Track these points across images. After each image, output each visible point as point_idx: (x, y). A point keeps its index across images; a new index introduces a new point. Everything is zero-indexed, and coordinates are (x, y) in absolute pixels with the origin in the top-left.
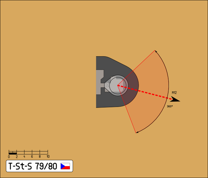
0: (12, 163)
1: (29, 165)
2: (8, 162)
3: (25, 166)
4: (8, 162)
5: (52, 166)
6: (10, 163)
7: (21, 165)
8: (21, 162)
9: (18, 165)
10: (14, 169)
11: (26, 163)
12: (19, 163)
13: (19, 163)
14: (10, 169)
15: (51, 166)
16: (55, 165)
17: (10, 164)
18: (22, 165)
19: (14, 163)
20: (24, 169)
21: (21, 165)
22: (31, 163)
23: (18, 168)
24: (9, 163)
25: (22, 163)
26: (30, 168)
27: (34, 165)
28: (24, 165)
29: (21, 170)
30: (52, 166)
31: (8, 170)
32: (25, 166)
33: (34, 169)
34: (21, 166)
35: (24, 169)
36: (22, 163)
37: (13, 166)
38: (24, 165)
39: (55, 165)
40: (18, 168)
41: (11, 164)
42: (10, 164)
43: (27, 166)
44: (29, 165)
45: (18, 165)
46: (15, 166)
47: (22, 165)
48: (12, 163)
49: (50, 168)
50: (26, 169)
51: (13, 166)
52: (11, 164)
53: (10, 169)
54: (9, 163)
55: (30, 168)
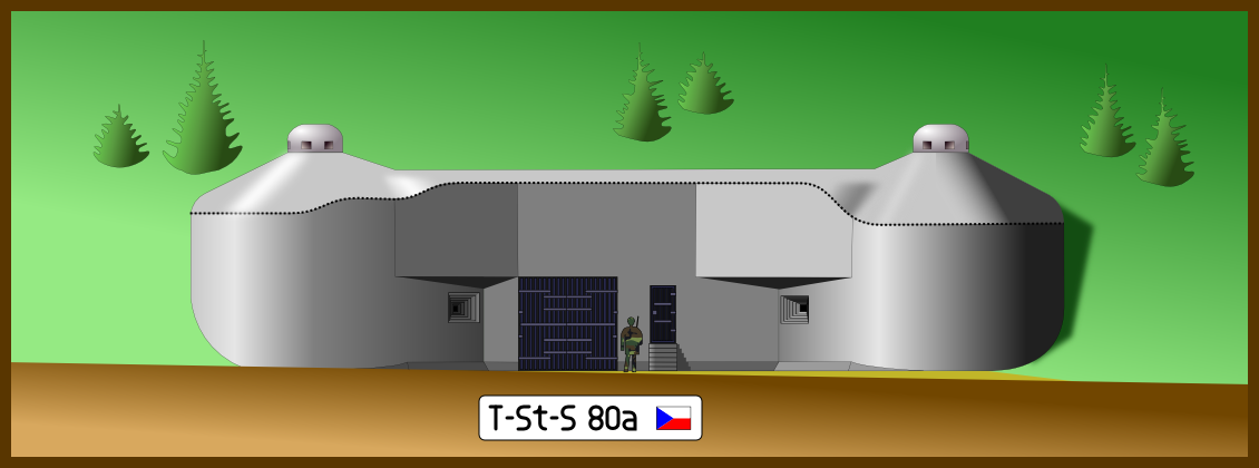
0: (501, 407)
1: (567, 412)
2: (486, 402)
3: (552, 418)
4: (486, 402)
5: (604, 418)
6: (496, 408)
7: (535, 412)
8: (535, 402)
9: (523, 412)
10: (508, 430)
11: (553, 404)
12: (529, 407)
13: (529, 407)
14: (496, 429)
15: (599, 418)
16: (613, 413)
17: (493, 410)
18: (540, 412)
19: (510, 404)
20: (545, 429)
21: (535, 412)
22: (574, 407)
23: (525, 424)
24: (490, 407)
25: (540, 407)
26: (569, 424)
27: (581, 416)
28: (546, 412)
29: (534, 433)
30: (604, 418)
31: (487, 431)
32: (552, 418)
33: (582, 431)
34: (534, 419)
35: (545, 429)
36: (540, 407)
37: (507, 418)
38: (546, 412)
39: (613, 413)
40: (525, 424)
41: (499, 410)
42: (493, 410)
43: (557, 418)
44: (567, 412)
45: (523, 412)
46: (512, 418)
47: (540, 412)
48: (501, 407)
49: (596, 423)
50: (554, 430)
51: (507, 418)
52: (499, 410)
53: (496, 429)
54: (490, 407)
55: (569, 424)
